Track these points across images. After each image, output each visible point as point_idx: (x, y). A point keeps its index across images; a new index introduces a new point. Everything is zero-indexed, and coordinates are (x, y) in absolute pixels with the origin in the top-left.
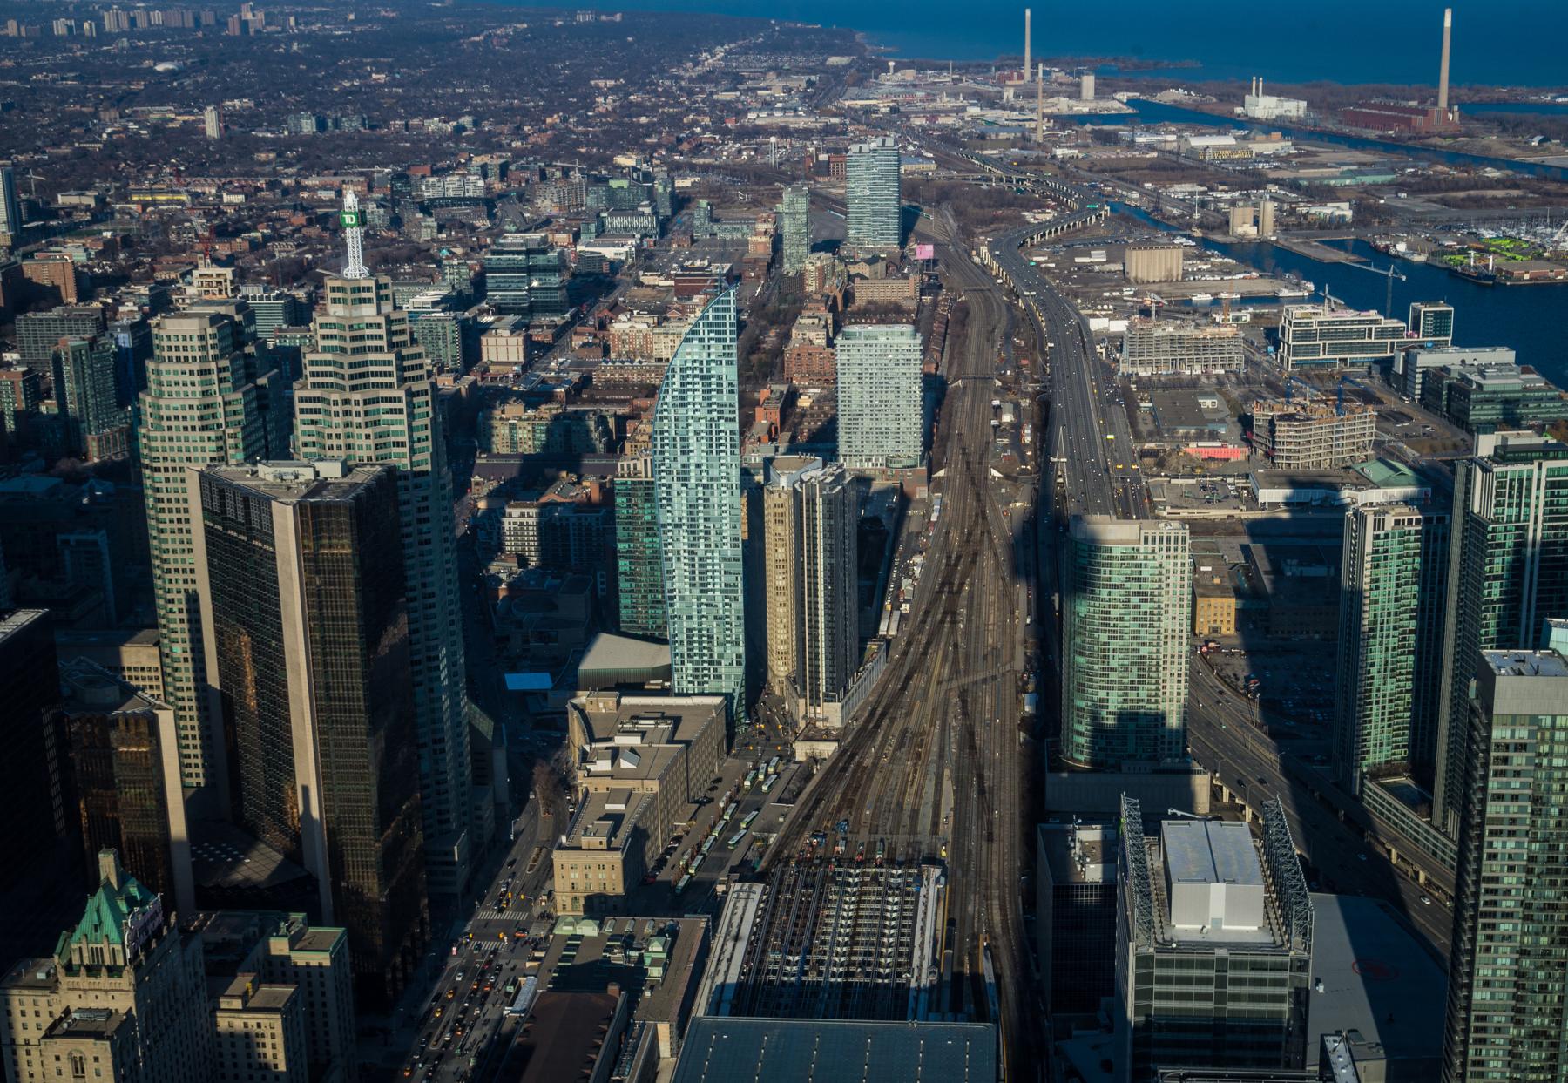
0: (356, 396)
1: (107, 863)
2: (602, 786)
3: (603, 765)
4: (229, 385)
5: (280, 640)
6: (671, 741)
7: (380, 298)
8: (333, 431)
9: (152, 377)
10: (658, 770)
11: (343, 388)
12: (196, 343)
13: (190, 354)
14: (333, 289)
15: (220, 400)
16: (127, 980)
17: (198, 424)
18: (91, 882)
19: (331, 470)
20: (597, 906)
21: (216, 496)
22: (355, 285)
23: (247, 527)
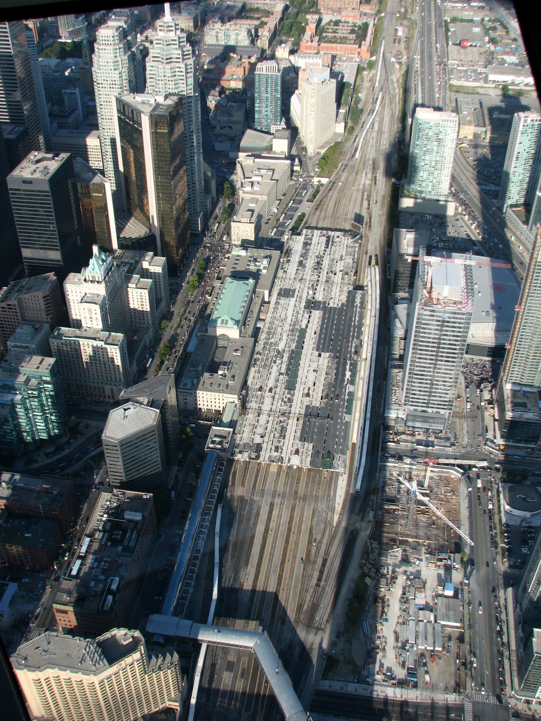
0: (168, 66)
1: (95, 249)
2: (248, 196)
3: (248, 189)
4: (122, 50)
5: (144, 159)
6: (272, 180)
7: (176, 29)
8: (160, 79)
9: (96, 50)
10: (267, 192)
11: (163, 63)
12: (112, 39)
13: (109, 43)
14: (160, 26)
15: (120, 59)
16: (103, 285)
17: (112, 68)
18: (90, 255)
19: (160, 99)
20: (245, 244)
21: (122, 107)
22: (168, 25)
23: (132, 119)
